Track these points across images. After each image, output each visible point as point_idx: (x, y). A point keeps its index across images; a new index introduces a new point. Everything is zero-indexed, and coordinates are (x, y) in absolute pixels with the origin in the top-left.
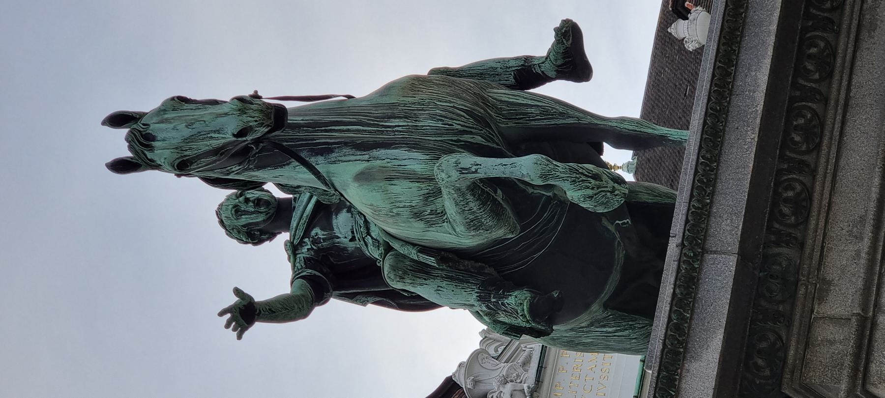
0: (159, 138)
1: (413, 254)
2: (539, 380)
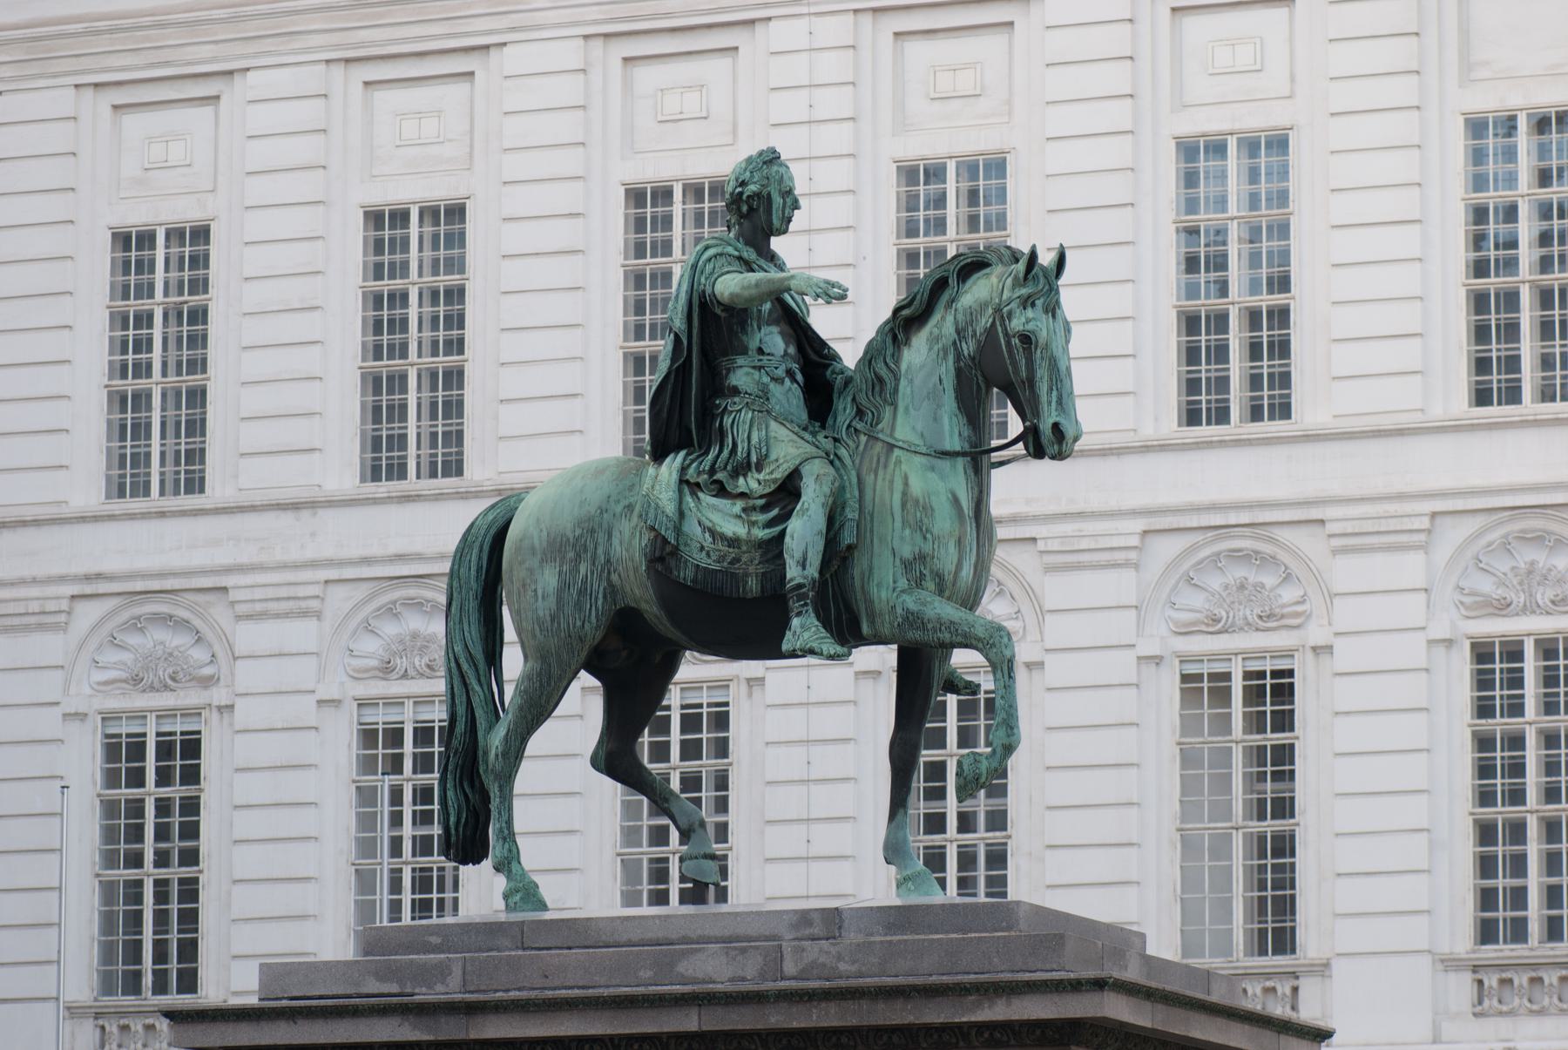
1: (851, 514)
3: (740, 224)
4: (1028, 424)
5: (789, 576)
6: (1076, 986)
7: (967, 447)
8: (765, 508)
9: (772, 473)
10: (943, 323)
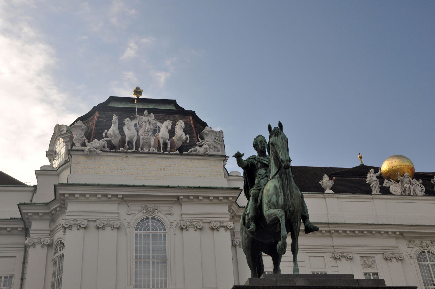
0: (278, 138)
1: (259, 199)
2: (211, 156)
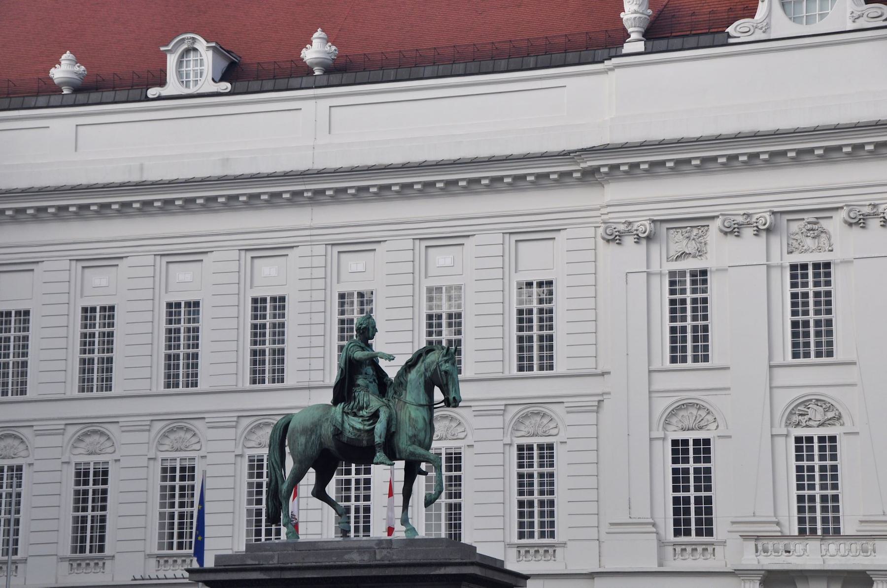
1: (394, 422)
3: (360, 336)
4: (446, 397)
5: (376, 441)
6: (465, 564)
7: (428, 404)
8: (368, 420)
9: (370, 410)
10: (421, 367)
